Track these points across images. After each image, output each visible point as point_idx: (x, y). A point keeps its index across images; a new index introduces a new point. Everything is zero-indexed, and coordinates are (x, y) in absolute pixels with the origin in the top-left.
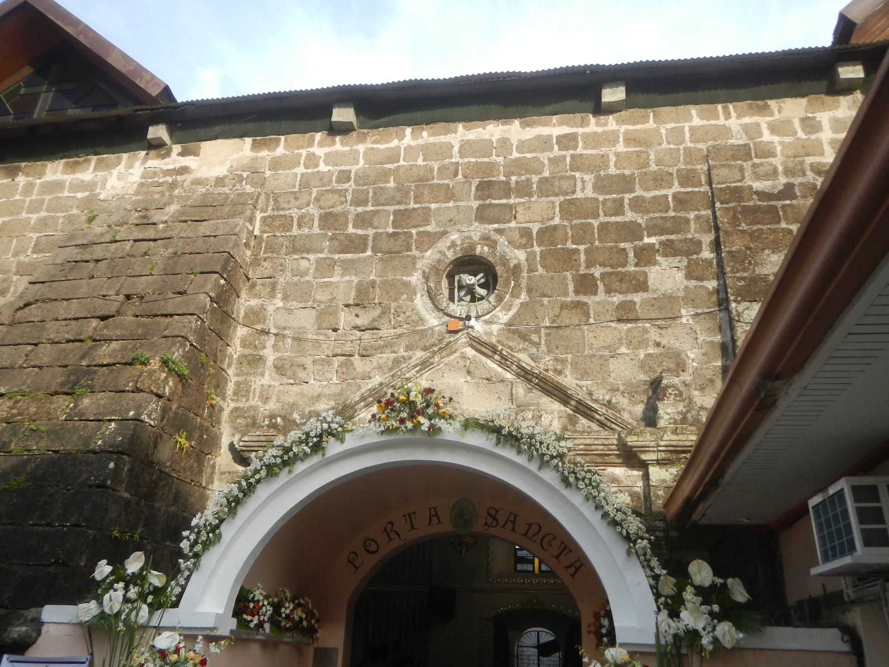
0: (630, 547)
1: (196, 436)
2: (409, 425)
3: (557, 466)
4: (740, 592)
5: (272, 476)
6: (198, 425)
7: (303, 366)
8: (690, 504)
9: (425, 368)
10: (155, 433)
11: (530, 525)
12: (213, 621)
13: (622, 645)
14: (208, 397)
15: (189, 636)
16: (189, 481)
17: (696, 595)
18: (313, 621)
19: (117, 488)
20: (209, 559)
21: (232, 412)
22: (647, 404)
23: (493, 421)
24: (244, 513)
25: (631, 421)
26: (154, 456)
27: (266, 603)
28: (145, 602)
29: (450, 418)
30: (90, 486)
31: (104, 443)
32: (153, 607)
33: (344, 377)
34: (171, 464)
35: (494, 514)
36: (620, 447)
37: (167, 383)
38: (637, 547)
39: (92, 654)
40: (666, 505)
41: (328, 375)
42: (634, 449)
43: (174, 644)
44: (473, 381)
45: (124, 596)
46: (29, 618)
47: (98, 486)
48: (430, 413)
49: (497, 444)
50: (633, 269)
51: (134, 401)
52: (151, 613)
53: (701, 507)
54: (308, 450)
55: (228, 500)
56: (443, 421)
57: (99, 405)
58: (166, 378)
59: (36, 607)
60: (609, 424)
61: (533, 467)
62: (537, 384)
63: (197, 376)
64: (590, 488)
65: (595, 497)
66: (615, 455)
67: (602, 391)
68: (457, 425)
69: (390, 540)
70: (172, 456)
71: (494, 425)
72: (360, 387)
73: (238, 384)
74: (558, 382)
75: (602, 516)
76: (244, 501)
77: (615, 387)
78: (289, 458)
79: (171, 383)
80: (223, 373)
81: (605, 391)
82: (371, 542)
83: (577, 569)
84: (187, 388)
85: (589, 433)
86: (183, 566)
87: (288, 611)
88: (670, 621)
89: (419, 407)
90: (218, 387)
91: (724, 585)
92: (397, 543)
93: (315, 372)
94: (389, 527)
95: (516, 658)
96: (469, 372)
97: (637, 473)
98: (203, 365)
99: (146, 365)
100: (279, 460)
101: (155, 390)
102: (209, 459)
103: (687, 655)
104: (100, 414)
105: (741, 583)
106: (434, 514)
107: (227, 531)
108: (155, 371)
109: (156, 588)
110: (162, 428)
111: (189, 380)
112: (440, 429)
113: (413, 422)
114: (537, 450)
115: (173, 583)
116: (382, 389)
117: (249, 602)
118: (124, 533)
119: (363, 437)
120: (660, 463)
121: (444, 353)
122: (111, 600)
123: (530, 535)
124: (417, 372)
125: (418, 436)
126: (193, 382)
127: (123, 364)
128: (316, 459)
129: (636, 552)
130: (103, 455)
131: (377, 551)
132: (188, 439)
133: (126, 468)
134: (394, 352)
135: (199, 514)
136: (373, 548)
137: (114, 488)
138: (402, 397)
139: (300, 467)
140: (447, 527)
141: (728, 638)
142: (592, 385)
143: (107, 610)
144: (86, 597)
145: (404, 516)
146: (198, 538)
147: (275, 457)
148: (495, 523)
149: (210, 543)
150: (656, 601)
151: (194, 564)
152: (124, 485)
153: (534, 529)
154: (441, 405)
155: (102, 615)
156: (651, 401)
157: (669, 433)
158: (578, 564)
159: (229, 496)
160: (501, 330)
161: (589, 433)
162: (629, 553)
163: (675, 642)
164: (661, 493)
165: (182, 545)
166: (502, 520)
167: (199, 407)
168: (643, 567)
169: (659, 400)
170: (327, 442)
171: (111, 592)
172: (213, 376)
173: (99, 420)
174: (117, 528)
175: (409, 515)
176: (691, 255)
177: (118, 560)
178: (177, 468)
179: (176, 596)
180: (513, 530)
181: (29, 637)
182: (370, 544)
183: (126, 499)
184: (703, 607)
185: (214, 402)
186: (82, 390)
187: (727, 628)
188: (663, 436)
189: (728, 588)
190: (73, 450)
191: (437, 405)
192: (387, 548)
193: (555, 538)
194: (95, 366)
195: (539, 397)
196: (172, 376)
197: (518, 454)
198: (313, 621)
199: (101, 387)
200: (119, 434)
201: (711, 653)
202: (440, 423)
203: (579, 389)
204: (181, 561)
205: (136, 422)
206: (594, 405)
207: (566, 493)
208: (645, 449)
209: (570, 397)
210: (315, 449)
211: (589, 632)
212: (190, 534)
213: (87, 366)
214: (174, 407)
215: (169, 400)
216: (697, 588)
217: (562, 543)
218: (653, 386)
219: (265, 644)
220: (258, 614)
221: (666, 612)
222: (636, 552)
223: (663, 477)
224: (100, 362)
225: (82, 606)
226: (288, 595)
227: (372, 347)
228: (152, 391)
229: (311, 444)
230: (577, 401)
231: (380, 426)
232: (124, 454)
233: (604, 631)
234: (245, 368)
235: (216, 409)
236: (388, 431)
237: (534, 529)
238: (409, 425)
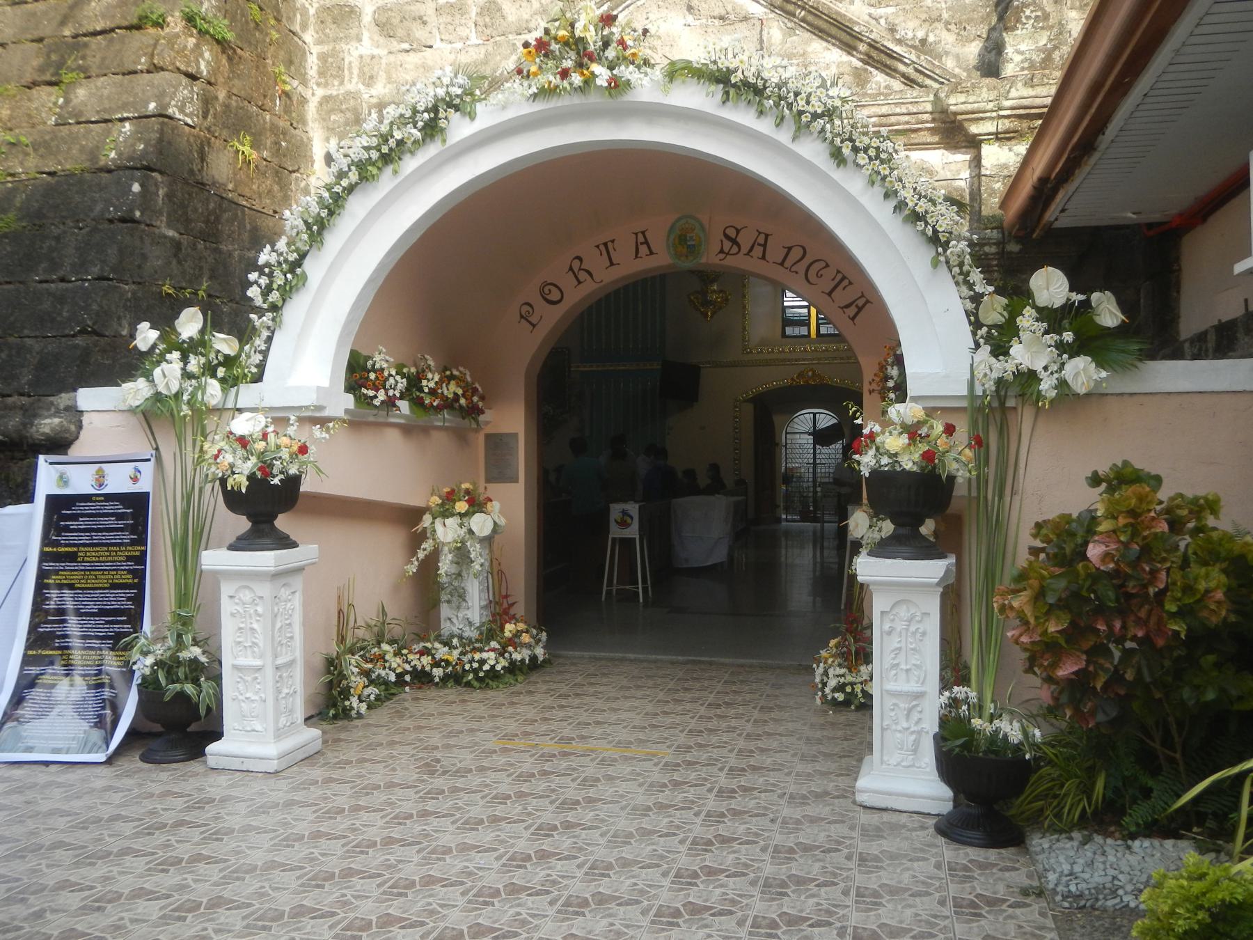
0: (938, 254)
1: (269, 142)
2: (577, 79)
3: (823, 130)
4: (1110, 312)
5: (367, 180)
6: (268, 126)
7: (420, 18)
8: (1045, 191)
10: (197, 137)
11: (790, 249)
12: (314, 396)
13: (916, 399)
14: (276, 78)
15: (280, 419)
16: (271, 213)
17: (1037, 320)
19: (154, 224)
20: (294, 311)
21: (321, 104)
22: (988, 38)
23: (715, 62)
24: (334, 240)
25: (957, 71)
26: (204, 173)
27: (393, 373)
28: (214, 375)
29: (645, 64)
30: (111, 221)
31: (120, 154)
32: (229, 383)
33: (488, 32)
34: (236, 186)
35: (734, 237)
36: (937, 116)
37: (201, 55)
38: (949, 252)
39: (157, 449)
40: (1004, 204)
41: (463, 32)
42: (959, 117)
43: (258, 428)
44: (698, 23)
45: (184, 369)
46: (62, 407)
47: (123, 220)
48: (610, 58)
49: (724, 102)
51: (152, 86)
52: (225, 391)
53: (1060, 197)
54: (418, 135)
55: (306, 222)
56: (631, 67)
57: (101, 96)
58: (197, 46)
59: (67, 392)
60: (920, 79)
61: (784, 136)
62: (803, 20)
63: (250, 43)
64: (877, 162)
65: (884, 179)
66: (929, 129)
67: (911, 24)
68: (657, 73)
69: (580, 282)
70: (235, 174)
71: (719, 70)
73: (323, 58)
74: (838, 13)
75: (895, 208)
76: (331, 223)
77: (935, 15)
78: (391, 149)
79: (207, 55)
80: (296, 39)
81: (916, 23)
82: (551, 287)
83: (860, 309)
84: (238, 64)
85: (886, 95)
86: (257, 324)
87: (432, 385)
88: (993, 360)
89: (591, 48)
90: (291, 62)
91: (1086, 304)
92: (589, 287)
93: (442, 27)
94: (576, 264)
95: (784, 449)
96: (690, 8)
97: (962, 158)
98: (257, 24)
99: (162, 28)
100: (375, 155)
101: (183, 67)
102: (297, 179)
103: (1015, 408)
104: (105, 110)
105: (1113, 299)
106: (642, 242)
107: (314, 268)
108: (177, 36)
109: (227, 357)
110: (208, 129)
111: (239, 51)
112: (628, 82)
113: (582, 74)
114: (790, 106)
115: (247, 347)
117: (369, 371)
118: (181, 288)
119: (504, 108)
120: (1000, 137)
122: (165, 376)
123: (787, 264)
125: (593, 99)
126: (246, 54)
127: (126, 28)
128: (432, 150)
129: (947, 262)
130: (121, 173)
131: (560, 301)
132: (256, 145)
133: (161, 192)
135: (268, 247)
136: (555, 295)
137: (148, 222)
138: (562, 33)
139: (410, 164)
140: (662, 259)
141: (1082, 378)
142: (896, 14)
143: (161, 388)
144: (133, 376)
145: (598, 247)
146: (271, 283)
147: (367, 149)
148: (735, 249)
149: (291, 288)
150: (974, 334)
151: (273, 319)
152: (164, 219)
154: (630, 43)
155: (158, 397)
156: (995, 35)
157: (1020, 85)
158: (860, 303)
159: (306, 216)
161: (886, 95)
162: (935, 264)
163: (997, 391)
164: (998, 186)
165: (250, 293)
167: (265, 96)
168: (957, 284)
169: (1006, 29)
170: (446, 118)
171: (164, 365)
172: (279, 44)
173: (106, 121)
174: (168, 282)
175: (605, 244)
177: (165, 320)
178: (247, 192)
179: (257, 366)
180: (763, 257)
181: (67, 431)
182: (550, 290)
183: (172, 239)
184: (1048, 336)
185: (288, 88)
186: (70, 75)
187: (1082, 366)
188: (1009, 92)
189: (1090, 307)
190: (76, 169)
191: (622, 42)
192: (576, 295)
193: (827, 266)
194: (85, 35)
195: (807, 43)
196: (208, 43)
197: (759, 117)
198: (475, 399)
199: (99, 67)
200: (139, 140)
201: (1052, 402)
202: (627, 72)
203: (874, 22)
204: (252, 316)
205: (161, 119)
206: (898, 49)
207: (837, 175)
208: (977, 116)
209: (857, 37)
210: (429, 132)
211: (870, 392)
212: (259, 277)
213: (74, 37)
214: (222, 95)
215: (209, 83)
216: (1040, 310)
217: (838, 272)
218: (999, 8)
219: (407, 430)
220: (384, 388)
221: (988, 348)
222: (947, 262)
223: (1003, 161)
224: (91, 29)
225: (127, 386)
226: (431, 363)
228: (178, 69)
229: (420, 124)
230: (870, 45)
231: (530, 86)
232: (153, 170)
233: (891, 384)
234: (331, 30)
235: (295, 99)
236: (546, 92)
237: (796, 254)
238: (577, 79)
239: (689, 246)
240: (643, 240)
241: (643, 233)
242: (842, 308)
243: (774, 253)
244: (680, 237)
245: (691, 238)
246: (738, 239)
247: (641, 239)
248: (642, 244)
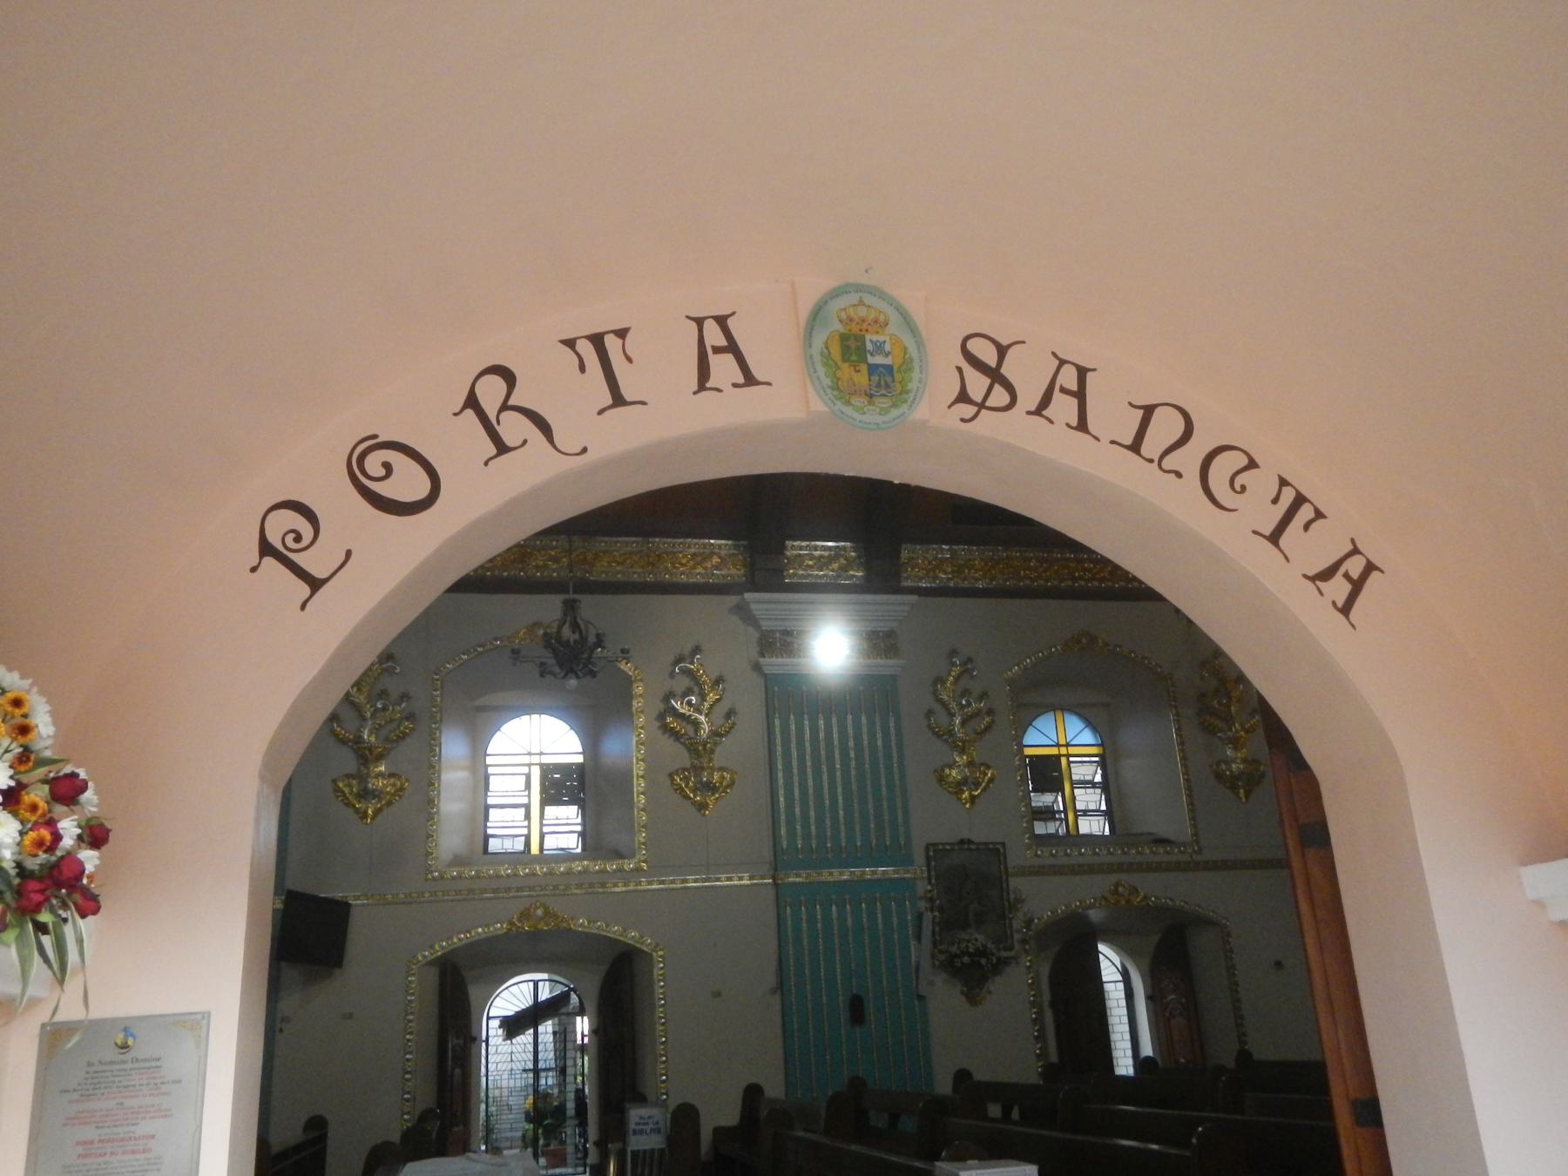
11: (1149, 411)
18: (69, 828)
35: (992, 362)
69: (502, 448)
83: (1357, 585)
94: (491, 392)
123: (1151, 446)
136: (407, 483)
145: (570, 343)
148: (999, 396)
153: (1165, 427)
158: (1355, 567)
175: (597, 340)
180: (1082, 426)
182: (387, 466)
193: (1252, 464)
217: (1283, 482)
237: (1165, 427)
239: (872, 369)
240: (723, 342)
241: (722, 321)
242: (1313, 579)
244: (844, 338)
245: (879, 348)
246: (1004, 371)
247: (714, 336)
248: (717, 350)
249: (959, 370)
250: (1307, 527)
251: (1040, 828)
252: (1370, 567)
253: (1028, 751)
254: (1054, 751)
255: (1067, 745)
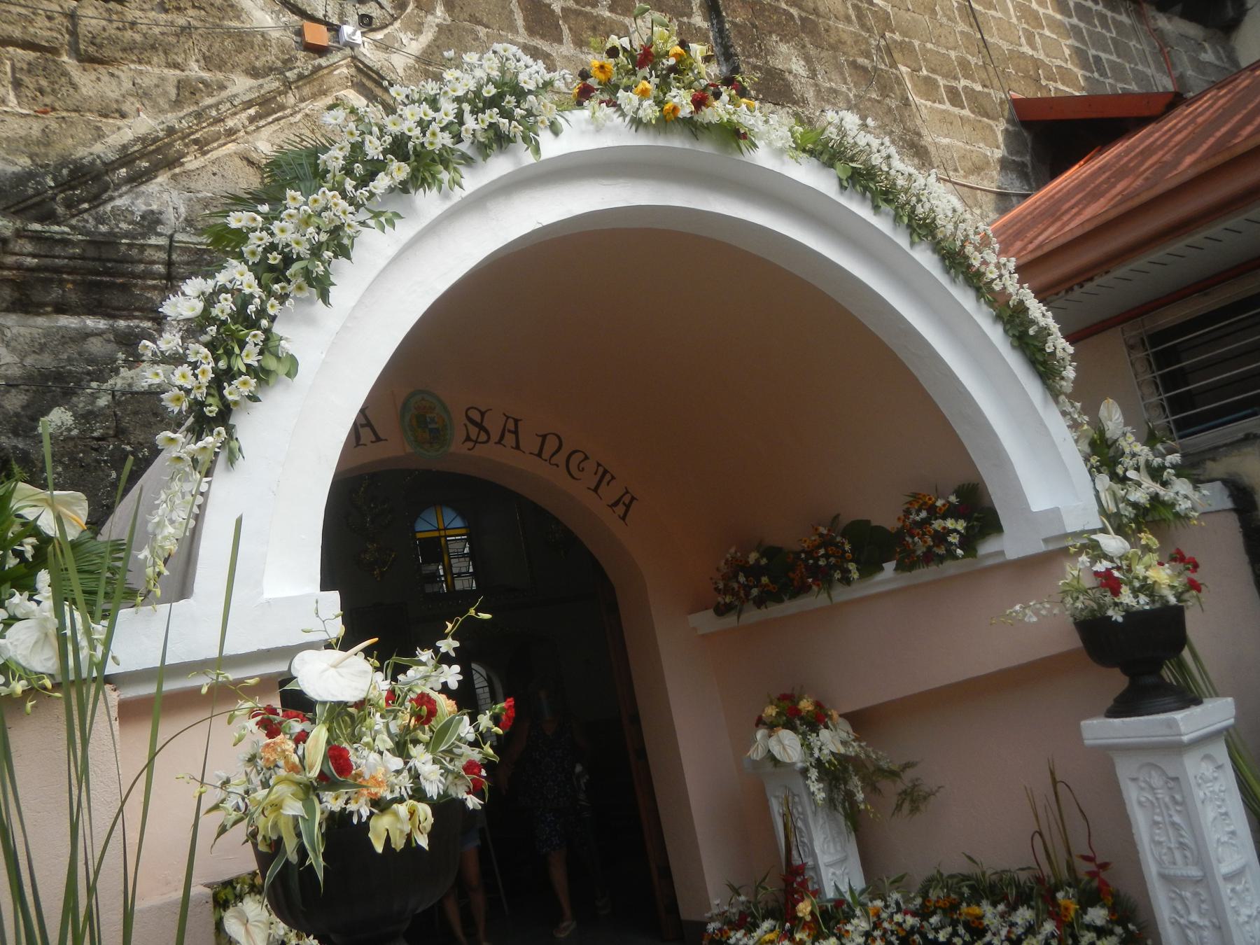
9: (269, 115)
11: (544, 437)
50: (607, 14)
72: (99, 135)
83: (628, 507)
116: (171, 145)
121: (307, 91)
123: (546, 455)
124: (252, 120)
134: (176, 66)
148: (483, 437)
158: (627, 499)
160: (410, 68)
166: (495, 429)
176: (682, 16)
180: (518, 447)
193: (586, 458)
217: (599, 465)
227: (113, 41)
243: (530, 442)
246: (484, 424)
249: (465, 425)
250: (608, 484)
251: (429, 589)
252: (633, 499)
253: (419, 536)
254: (436, 534)
255: (445, 529)
